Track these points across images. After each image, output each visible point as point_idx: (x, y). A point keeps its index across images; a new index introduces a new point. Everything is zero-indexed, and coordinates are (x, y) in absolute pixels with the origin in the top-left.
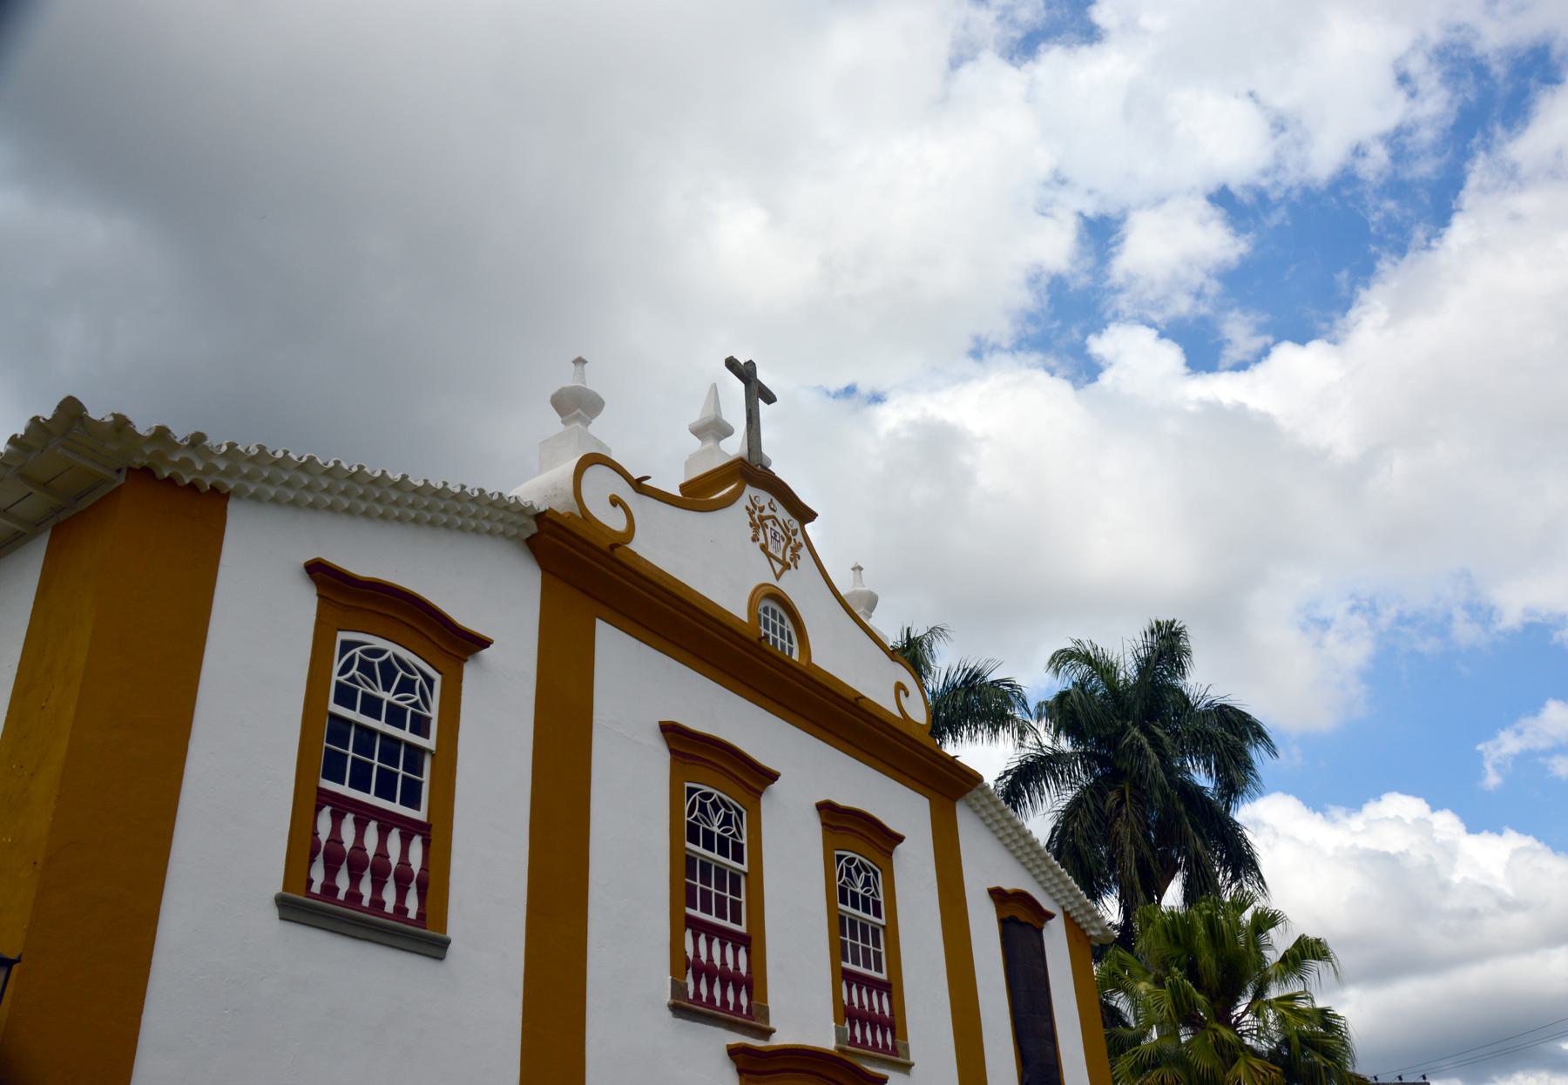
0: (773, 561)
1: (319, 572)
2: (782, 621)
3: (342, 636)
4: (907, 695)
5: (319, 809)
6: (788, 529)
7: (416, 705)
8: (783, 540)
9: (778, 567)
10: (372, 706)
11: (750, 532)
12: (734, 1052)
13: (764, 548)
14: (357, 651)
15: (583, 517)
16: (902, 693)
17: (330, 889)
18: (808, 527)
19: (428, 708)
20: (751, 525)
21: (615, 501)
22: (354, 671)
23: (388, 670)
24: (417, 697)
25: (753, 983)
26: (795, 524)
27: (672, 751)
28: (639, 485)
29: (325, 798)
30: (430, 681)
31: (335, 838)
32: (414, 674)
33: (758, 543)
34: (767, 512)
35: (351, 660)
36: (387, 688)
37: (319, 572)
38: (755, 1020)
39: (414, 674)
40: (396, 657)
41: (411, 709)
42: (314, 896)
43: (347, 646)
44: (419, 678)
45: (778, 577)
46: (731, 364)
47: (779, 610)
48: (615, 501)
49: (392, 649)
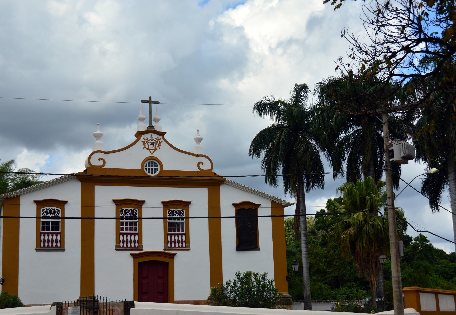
0: (150, 150)
1: (35, 201)
2: (154, 163)
3: (41, 209)
4: (203, 164)
5: (41, 235)
6: (157, 140)
7: (56, 215)
8: (155, 143)
9: (152, 151)
10: (48, 218)
11: (143, 146)
12: (131, 254)
13: (147, 149)
14: (45, 210)
15: (91, 167)
16: (201, 165)
17: (44, 246)
18: (165, 136)
19: (59, 215)
20: (143, 145)
21: (99, 159)
22: (45, 214)
23: (51, 212)
24: (57, 214)
25: (140, 241)
26: (160, 137)
27: (116, 204)
28: (106, 153)
29: (41, 233)
30: (59, 210)
31: (44, 239)
32: (55, 210)
33: (146, 148)
34: (150, 138)
35: (44, 212)
36: (51, 214)
37: (35, 201)
38: (140, 247)
39: (55, 210)
40: (52, 209)
41: (55, 216)
42: (42, 247)
43: (43, 210)
44: (56, 210)
45: (152, 154)
46: (143, 101)
47: (153, 161)
48: (99, 159)
49: (51, 208)
